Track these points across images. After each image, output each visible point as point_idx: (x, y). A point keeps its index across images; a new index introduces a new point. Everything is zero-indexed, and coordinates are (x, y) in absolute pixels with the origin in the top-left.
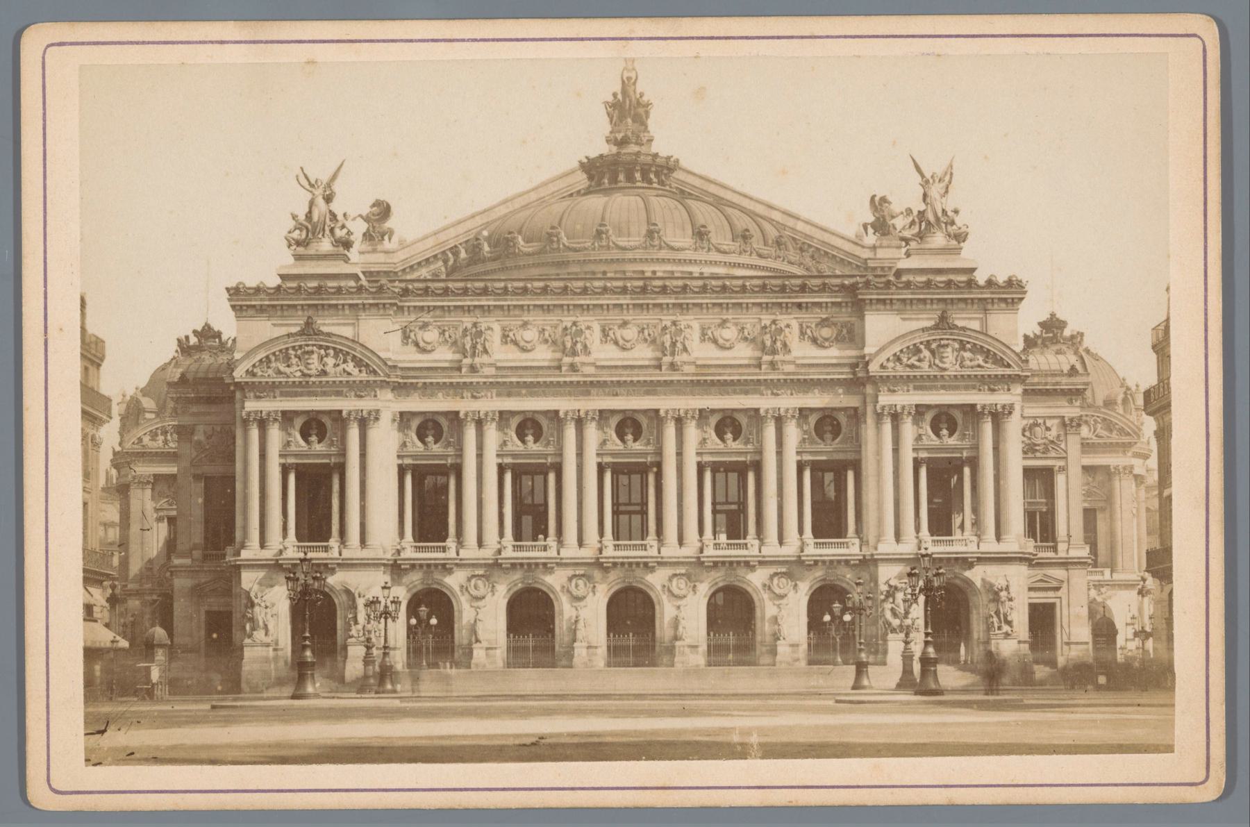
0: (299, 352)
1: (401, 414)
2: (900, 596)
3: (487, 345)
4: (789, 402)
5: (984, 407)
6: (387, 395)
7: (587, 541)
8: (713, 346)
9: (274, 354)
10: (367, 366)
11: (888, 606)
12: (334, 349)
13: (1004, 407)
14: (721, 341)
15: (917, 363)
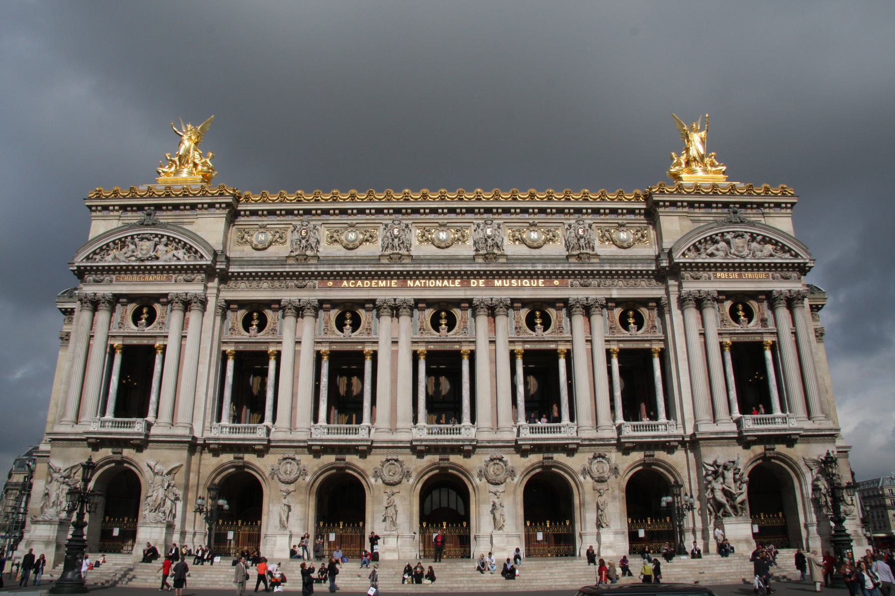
0: (137, 240)
1: (229, 303)
2: (729, 475)
3: (312, 241)
4: (594, 293)
5: (781, 293)
6: (215, 284)
7: (399, 425)
8: (524, 246)
9: (114, 242)
10: (196, 252)
11: (718, 485)
12: (168, 237)
13: (798, 292)
14: (528, 242)
15: (715, 252)
